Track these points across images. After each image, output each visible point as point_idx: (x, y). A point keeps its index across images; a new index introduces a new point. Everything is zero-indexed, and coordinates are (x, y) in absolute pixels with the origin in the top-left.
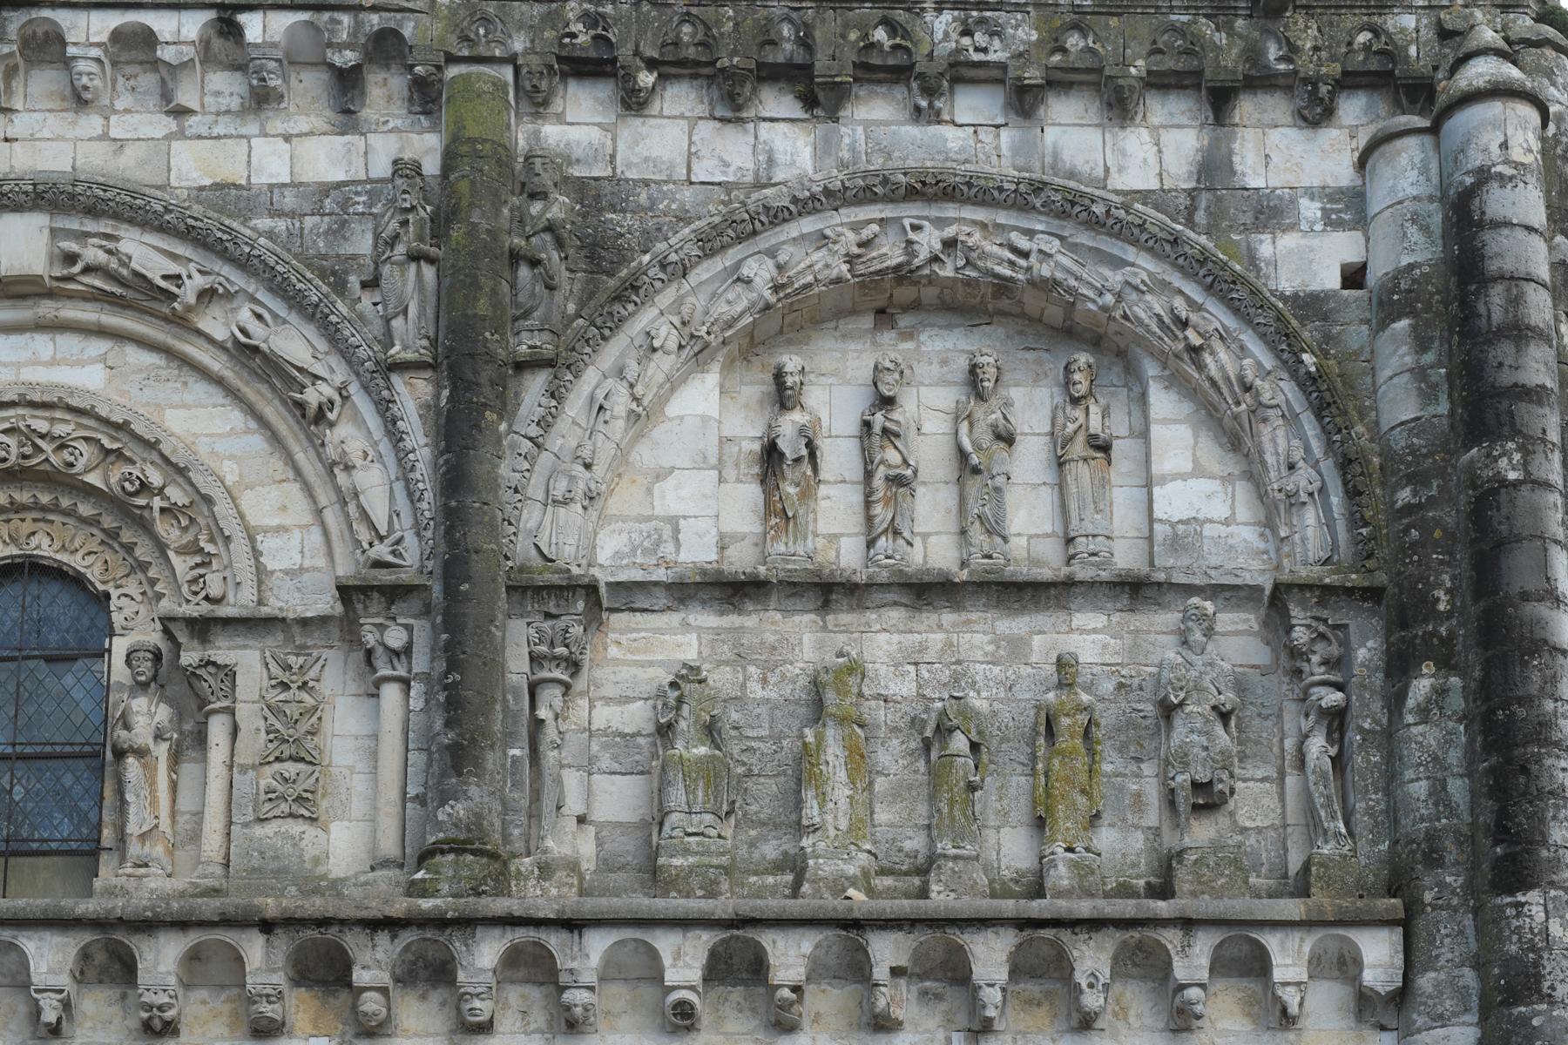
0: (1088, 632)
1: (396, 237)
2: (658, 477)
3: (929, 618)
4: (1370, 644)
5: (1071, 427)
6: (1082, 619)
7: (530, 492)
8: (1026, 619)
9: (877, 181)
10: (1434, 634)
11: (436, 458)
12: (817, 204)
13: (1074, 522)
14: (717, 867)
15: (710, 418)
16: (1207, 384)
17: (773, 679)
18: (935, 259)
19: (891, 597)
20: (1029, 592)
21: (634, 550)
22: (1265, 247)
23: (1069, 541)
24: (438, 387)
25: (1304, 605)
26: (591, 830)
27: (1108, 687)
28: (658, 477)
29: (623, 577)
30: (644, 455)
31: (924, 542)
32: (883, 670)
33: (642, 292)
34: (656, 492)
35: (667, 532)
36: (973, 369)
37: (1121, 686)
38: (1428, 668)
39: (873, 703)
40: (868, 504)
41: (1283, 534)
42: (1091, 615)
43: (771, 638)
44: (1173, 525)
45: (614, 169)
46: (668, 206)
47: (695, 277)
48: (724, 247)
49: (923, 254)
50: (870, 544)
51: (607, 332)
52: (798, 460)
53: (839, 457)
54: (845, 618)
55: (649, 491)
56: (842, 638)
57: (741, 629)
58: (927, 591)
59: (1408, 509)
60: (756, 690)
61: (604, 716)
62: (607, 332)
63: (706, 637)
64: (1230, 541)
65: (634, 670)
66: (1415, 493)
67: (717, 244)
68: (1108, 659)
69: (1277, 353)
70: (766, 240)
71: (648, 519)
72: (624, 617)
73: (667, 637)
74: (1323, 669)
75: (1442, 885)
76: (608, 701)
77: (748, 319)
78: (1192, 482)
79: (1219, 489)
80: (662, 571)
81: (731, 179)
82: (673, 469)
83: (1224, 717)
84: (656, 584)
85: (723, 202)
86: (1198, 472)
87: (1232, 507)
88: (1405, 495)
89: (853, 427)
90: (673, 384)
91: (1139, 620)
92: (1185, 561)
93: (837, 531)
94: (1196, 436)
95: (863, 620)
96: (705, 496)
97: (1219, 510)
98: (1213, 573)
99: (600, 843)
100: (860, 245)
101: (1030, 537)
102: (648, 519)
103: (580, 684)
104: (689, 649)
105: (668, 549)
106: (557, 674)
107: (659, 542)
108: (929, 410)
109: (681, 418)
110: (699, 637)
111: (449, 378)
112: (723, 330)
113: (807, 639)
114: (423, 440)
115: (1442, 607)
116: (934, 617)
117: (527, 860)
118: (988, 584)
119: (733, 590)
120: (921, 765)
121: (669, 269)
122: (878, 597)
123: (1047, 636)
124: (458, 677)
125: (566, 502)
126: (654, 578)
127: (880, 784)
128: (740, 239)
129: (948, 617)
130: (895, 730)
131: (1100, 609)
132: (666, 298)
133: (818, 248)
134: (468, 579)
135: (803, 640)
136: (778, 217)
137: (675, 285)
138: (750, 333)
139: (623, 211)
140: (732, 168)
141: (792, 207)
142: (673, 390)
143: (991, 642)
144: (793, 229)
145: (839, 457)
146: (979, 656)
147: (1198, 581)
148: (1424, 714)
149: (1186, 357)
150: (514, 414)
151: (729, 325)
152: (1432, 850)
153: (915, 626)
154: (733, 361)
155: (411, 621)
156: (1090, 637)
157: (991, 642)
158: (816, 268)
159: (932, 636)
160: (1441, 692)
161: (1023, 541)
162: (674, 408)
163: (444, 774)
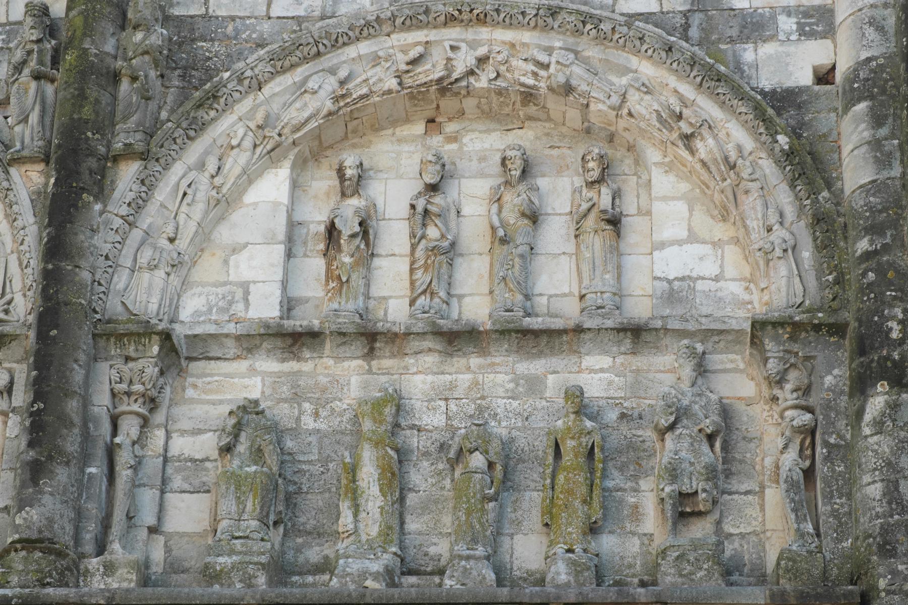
0: (596, 372)
1: (24, 63)
2: (234, 250)
3: (459, 362)
4: (836, 372)
5: (585, 206)
6: (590, 361)
7: (121, 261)
8: (543, 361)
9: (422, 10)
10: (888, 358)
11: (40, 232)
12: (372, 31)
13: (586, 282)
14: (256, 564)
15: (280, 203)
16: (698, 166)
17: (323, 413)
18: (471, 73)
19: (428, 344)
20: (544, 340)
21: (210, 310)
22: (748, 54)
23: (582, 297)
24: (48, 177)
25: (776, 339)
26: (161, 539)
27: (612, 416)
28: (234, 250)
29: (198, 330)
30: (225, 234)
31: (459, 302)
32: (418, 405)
33: (222, 100)
34: (231, 263)
35: (239, 294)
36: (504, 161)
37: (623, 416)
38: (882, 387)
39: (408, 432)
40: (412, 271)
41: (763, 286)
42: (598, 357)
43: (323, 380)
44: (670, 282)
45: (207, 9)
46: (250, 36)
47: (267, 90)
48: (293, 66)
49: (460, 69)
50: (412, 303)
51: (192, 133)
52: (353, 236)
53: (394, 236)
54: (387, 363)
55: (226, 262)
56: (384, 379)
57: (299, 373)
58: (458, 338)
59: (867, 256)
60: (309, 423)
61: (181, 445)
62: (192, 133)
63: (268, 380)
64: (719, 294)
65: (206, 407)
66: (871, 242)
67: (287, 63)
68: (612, 393)
69: (756, 136)
70: (328, 60)
71: (225, 284)
72: (201, 364)
73: (236, 380)
74: (795, 395)
75: (894, 573)
76: (183, 433)
77: (313, 124)
78: (687, 247)
79: (711, 252)
80: (232, 325)
81: (302, 13)
82: (246, 245)
83: (711, 438)
84: (227, 336)
85: (295, 32)
86: (693, 238)
87: (721, 266)
88: (863, 245)
89: (405, 211)
90: (249, 177)
91: (639, 362)
92: (679, 311)
93: (386, 295)
94: (691, 210)
95: (403, 364)
96: (272, 265)
97: (710, 268)
98: (703, 320)
99: (168, 550)
100: (408, 64)
101: (551, 296)
102: (225, 284)
103: (159, 417)
104: (254, 388)
105: (238, 308)
106: (136, 407)
107: (231, 303)
108: (473, 201)
109: (256, 204)
110: (263, 380)
111: (56, 170)
112: (293, 132)
113: (355, 380)
114: (32, 220)
115: (895, 335)
116: (463, 361)
117: (95, 560)
118: (509, 331)
119: (293, 339)
120: (447, 483)
121: (246, 82)
122: (415, 344)
123: (555, 374)
124: (42, 406)
125: (152, 267)
126: (225, 331)
127: (412, 499)
128: (306, 60)
129: (475, 361)
130: (426, 454)
131: (606, 352)
132: (244, 106)
133: (374, 66)
134: (56, 327)
135: (347, 378)
136: (338, 42)
137: (251, 97)
138: (317, 135)
139: (212, 40)
140: (304, 6)
141: (350, 33)
142: (250, 182)
143: (511, 381)
144: (351, 51)
145: (394, 236)
146: (501, 392)
147: (691, 326)
148: (879, 426)
149: (680, 143)
150: (109, 197)
151: (297, 129)
152: (886, 543)
153: (447, 368)
154: (305, 161)
155: (15, 365)
156: (598, 374)
157: (511, 381)
158: (371, 82)
159: (461, 376)
160: (894, 407)
161: (544, 300)
162: (251, 196)
163: (23, 485)
